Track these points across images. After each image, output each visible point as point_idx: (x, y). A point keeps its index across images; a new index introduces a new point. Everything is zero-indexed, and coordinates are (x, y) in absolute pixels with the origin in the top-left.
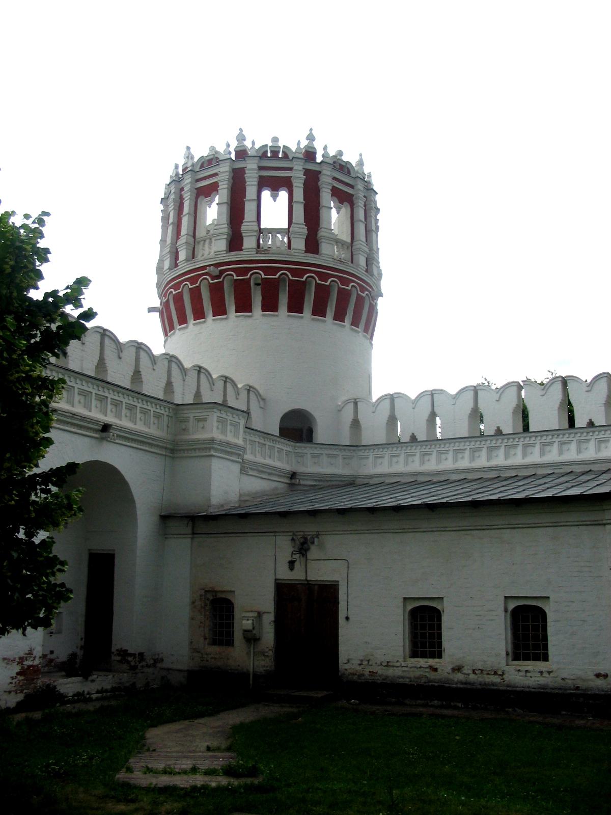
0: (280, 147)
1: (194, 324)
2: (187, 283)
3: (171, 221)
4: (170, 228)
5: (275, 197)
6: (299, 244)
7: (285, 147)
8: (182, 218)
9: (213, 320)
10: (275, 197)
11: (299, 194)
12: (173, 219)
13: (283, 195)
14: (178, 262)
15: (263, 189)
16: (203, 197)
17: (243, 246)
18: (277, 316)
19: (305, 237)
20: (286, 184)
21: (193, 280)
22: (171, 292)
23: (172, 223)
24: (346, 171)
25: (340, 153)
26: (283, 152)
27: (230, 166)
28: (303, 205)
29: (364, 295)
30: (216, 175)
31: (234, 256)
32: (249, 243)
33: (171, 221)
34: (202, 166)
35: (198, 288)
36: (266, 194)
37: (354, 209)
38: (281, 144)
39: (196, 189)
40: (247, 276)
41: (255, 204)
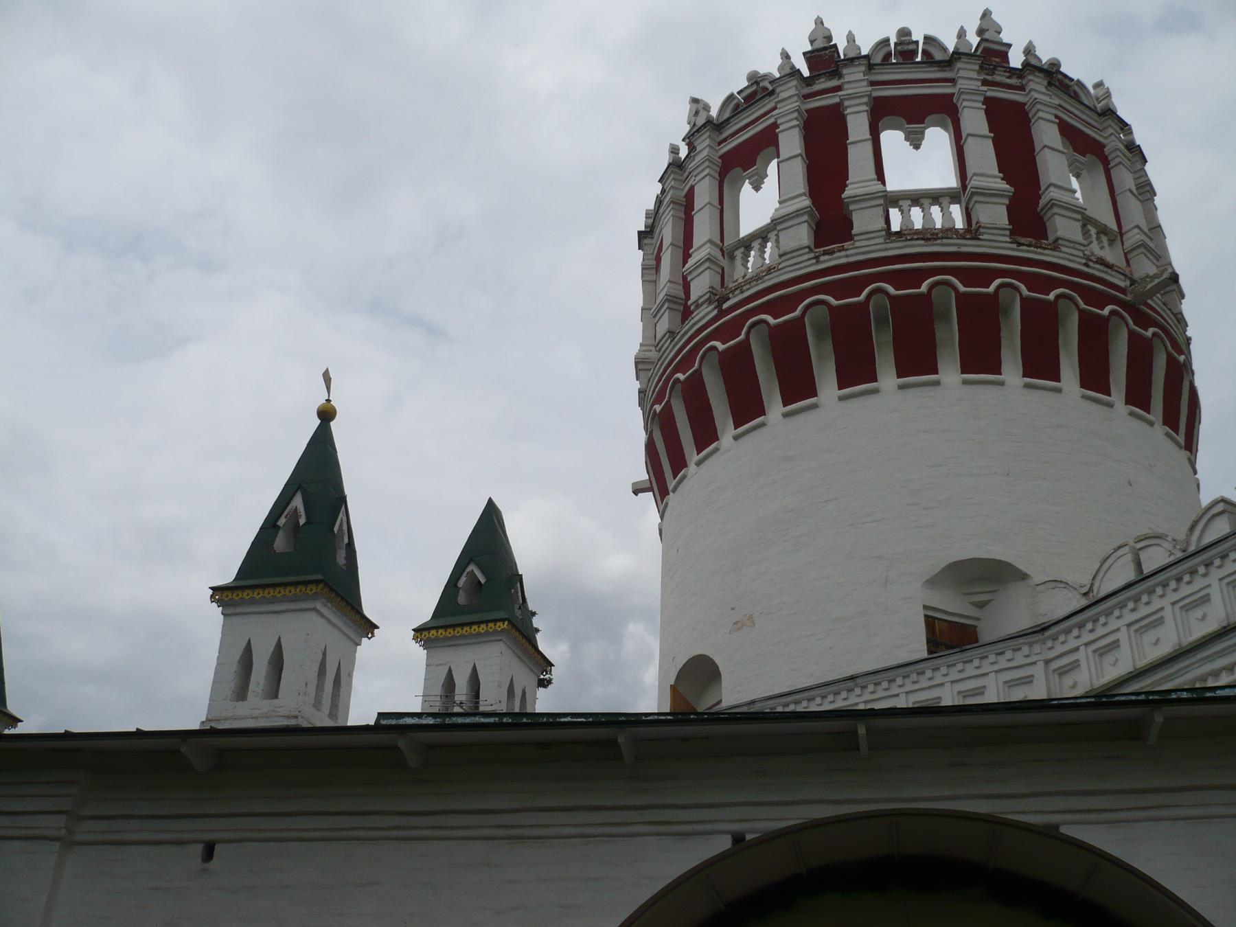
0: (917, 42)
2: (713, 343)
5: (915, 141)
6: (995, 215)
7: (928, 39)
8: (693, 216)
10: (915, 141)
11: (974, 120)
15: (886, 119)
16: (738, 170)
17: (852, 228)
26: (924, 52)
28: (990, 143)
32: (864, 221)
36: (893, 140)
37: (1112, 171)
39: (720, 157)
41: (868, 147)
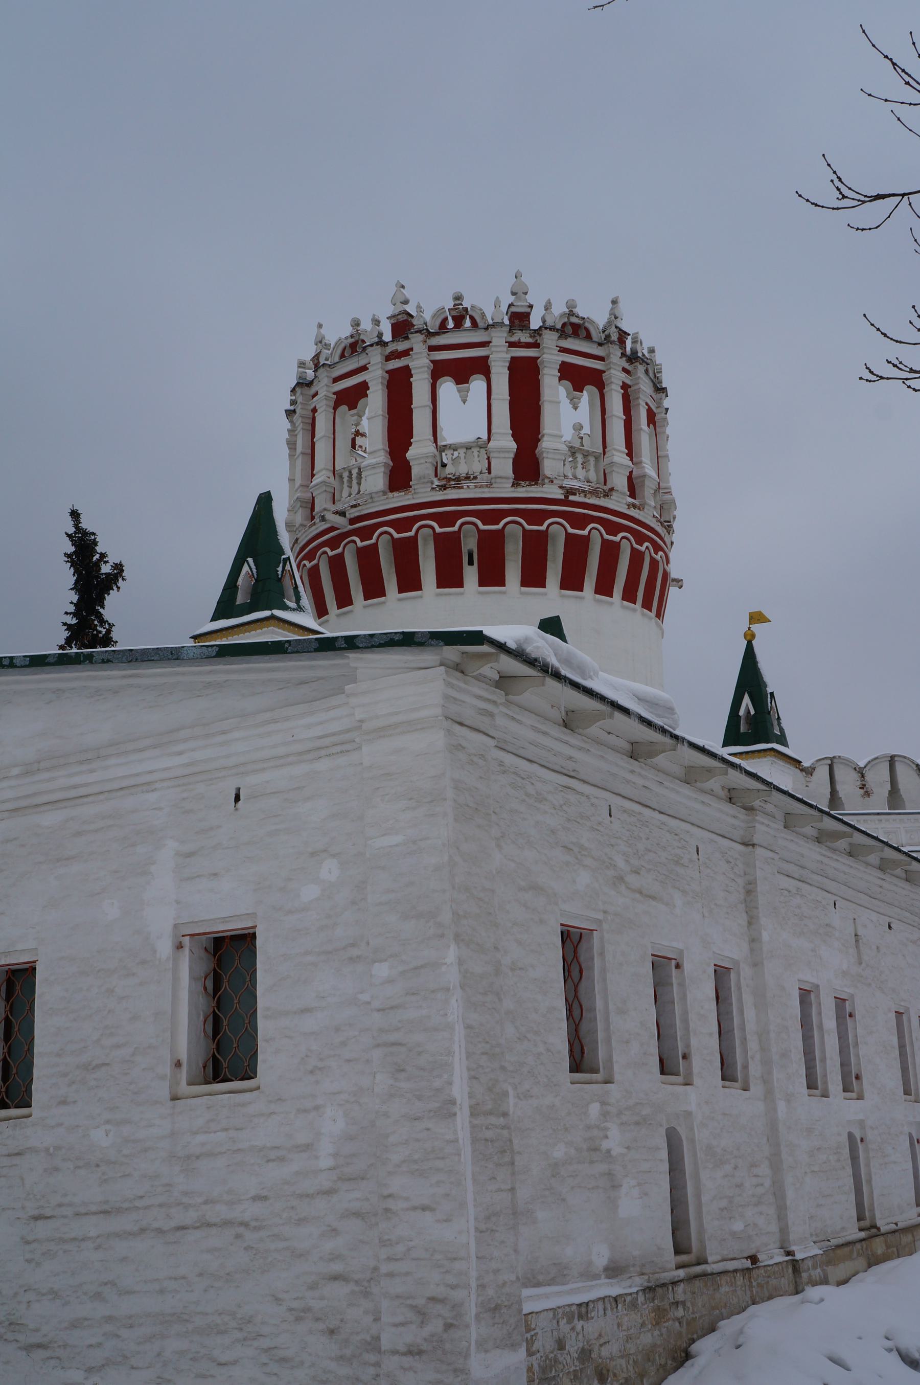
1: (338, 616)
3: (299, 449)
4: (299, 462)
6: (504, 467)
9: (365, 607)
12: (303, 447)
13: (478, 385)
14: (314, 513)
18: (504, 593)
19: (512, 456)
20: (482, 367)
21: (333, 543)
22: (305, 565)
23: (303, 453)
24: (584, 334)
25: (571, 305)
27: (381, 354)
29: (643, 549)
30: (364, 368)
31: (399, 499)
33: (299, 449)
34: (342, 356)
35: (341, 556)
38: (466, 303)
40: (454, 526)
